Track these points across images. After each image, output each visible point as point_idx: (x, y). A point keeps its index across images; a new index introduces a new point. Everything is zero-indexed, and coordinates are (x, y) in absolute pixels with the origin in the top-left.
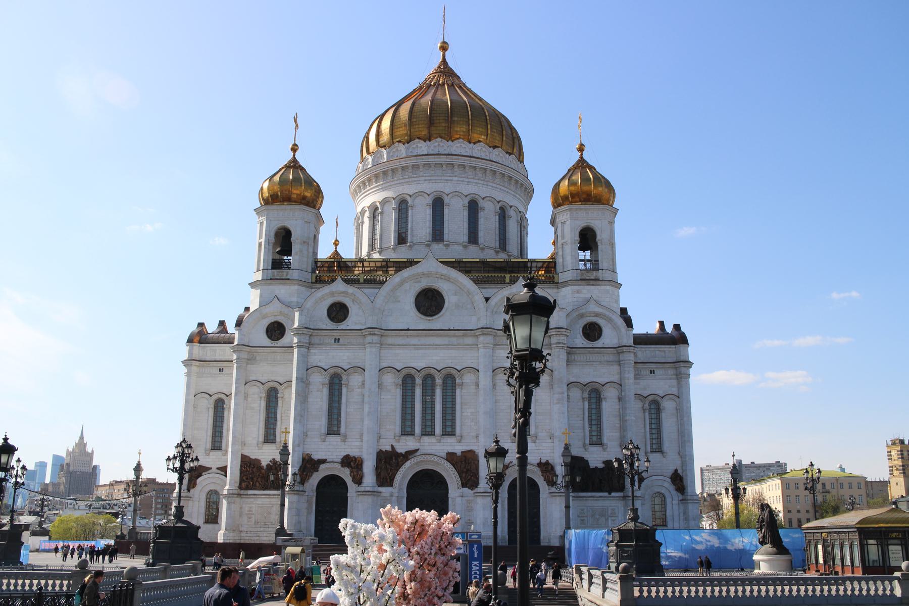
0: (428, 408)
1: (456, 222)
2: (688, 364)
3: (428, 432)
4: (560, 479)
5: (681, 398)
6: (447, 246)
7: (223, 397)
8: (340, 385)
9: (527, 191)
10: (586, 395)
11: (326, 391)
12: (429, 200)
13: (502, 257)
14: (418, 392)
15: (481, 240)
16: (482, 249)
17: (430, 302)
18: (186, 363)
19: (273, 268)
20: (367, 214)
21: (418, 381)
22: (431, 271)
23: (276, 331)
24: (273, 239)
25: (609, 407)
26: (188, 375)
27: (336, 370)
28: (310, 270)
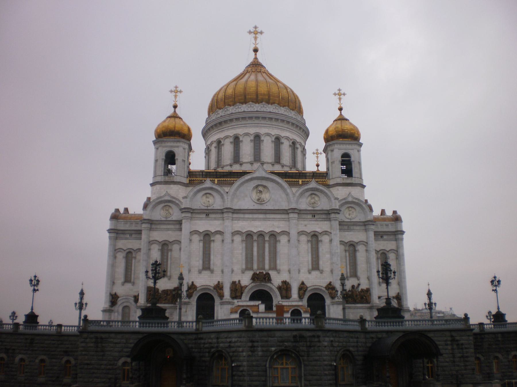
1: (268, 151)
2: (402, 233)
4: (339, 293)
5: (398, 253)
6: (263, 164)
8: (210, 241)
9: (306, 133)
10: (347, 248)
12: (252, 138)
13: (294, 171)
15: (282, 162)
18: (110, 231)
19: (164, 175)
20: (214, 145)
21: (255, 238)
24: (164, 157)
25: (361, 256)
26: (110, 238)
27: (207, 232)
28: (186, 176)
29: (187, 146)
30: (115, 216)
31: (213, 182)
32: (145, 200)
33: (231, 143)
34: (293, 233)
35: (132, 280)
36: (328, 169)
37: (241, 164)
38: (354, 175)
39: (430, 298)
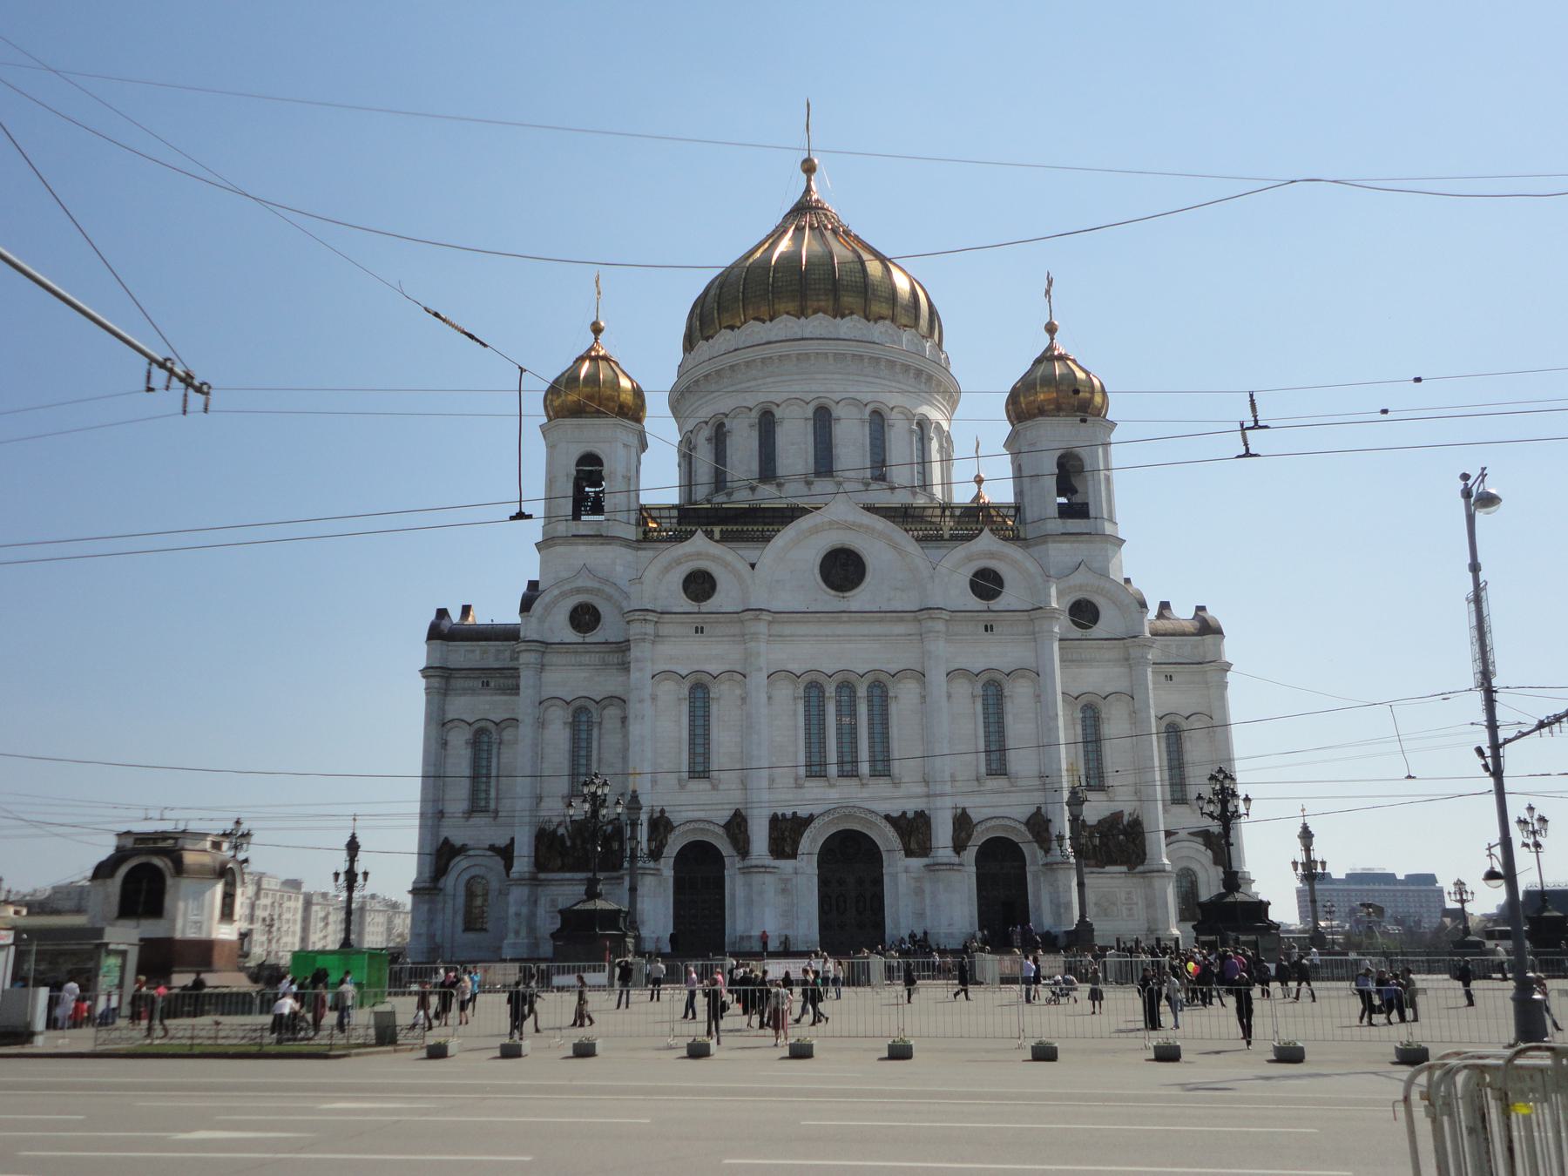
0: (848, 735)
2: (1227, 667)
3: (849, 770)
7: (491, 726)
11: (685, 708)
12: (810, 412)
14: (831, 709)
16: (893, 489)
17: (843, 569)
20: (706, 432)
21: (830, 691)
22: (838, 519)
23: (585, 618)
26: (429, 690)
29: (634, 441)
30: (441, 631)
31: (709, 535)
32: (524, 588)
33: (751, 426)
34: (937, 677)
35: (492, 806)
36: (1019, 493)
37: (780, 485)
38: (1092, 513)
39: (1308, 849)
